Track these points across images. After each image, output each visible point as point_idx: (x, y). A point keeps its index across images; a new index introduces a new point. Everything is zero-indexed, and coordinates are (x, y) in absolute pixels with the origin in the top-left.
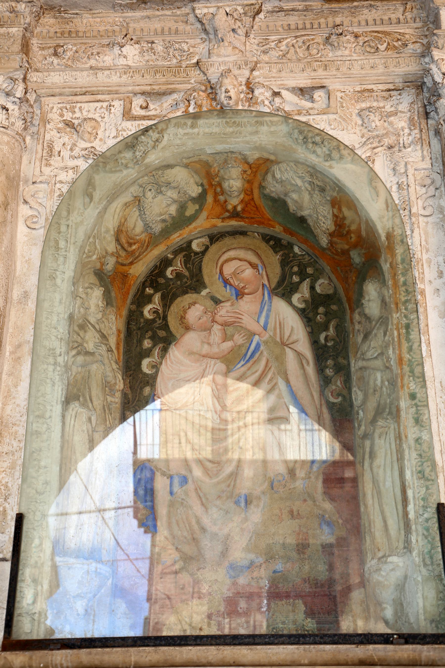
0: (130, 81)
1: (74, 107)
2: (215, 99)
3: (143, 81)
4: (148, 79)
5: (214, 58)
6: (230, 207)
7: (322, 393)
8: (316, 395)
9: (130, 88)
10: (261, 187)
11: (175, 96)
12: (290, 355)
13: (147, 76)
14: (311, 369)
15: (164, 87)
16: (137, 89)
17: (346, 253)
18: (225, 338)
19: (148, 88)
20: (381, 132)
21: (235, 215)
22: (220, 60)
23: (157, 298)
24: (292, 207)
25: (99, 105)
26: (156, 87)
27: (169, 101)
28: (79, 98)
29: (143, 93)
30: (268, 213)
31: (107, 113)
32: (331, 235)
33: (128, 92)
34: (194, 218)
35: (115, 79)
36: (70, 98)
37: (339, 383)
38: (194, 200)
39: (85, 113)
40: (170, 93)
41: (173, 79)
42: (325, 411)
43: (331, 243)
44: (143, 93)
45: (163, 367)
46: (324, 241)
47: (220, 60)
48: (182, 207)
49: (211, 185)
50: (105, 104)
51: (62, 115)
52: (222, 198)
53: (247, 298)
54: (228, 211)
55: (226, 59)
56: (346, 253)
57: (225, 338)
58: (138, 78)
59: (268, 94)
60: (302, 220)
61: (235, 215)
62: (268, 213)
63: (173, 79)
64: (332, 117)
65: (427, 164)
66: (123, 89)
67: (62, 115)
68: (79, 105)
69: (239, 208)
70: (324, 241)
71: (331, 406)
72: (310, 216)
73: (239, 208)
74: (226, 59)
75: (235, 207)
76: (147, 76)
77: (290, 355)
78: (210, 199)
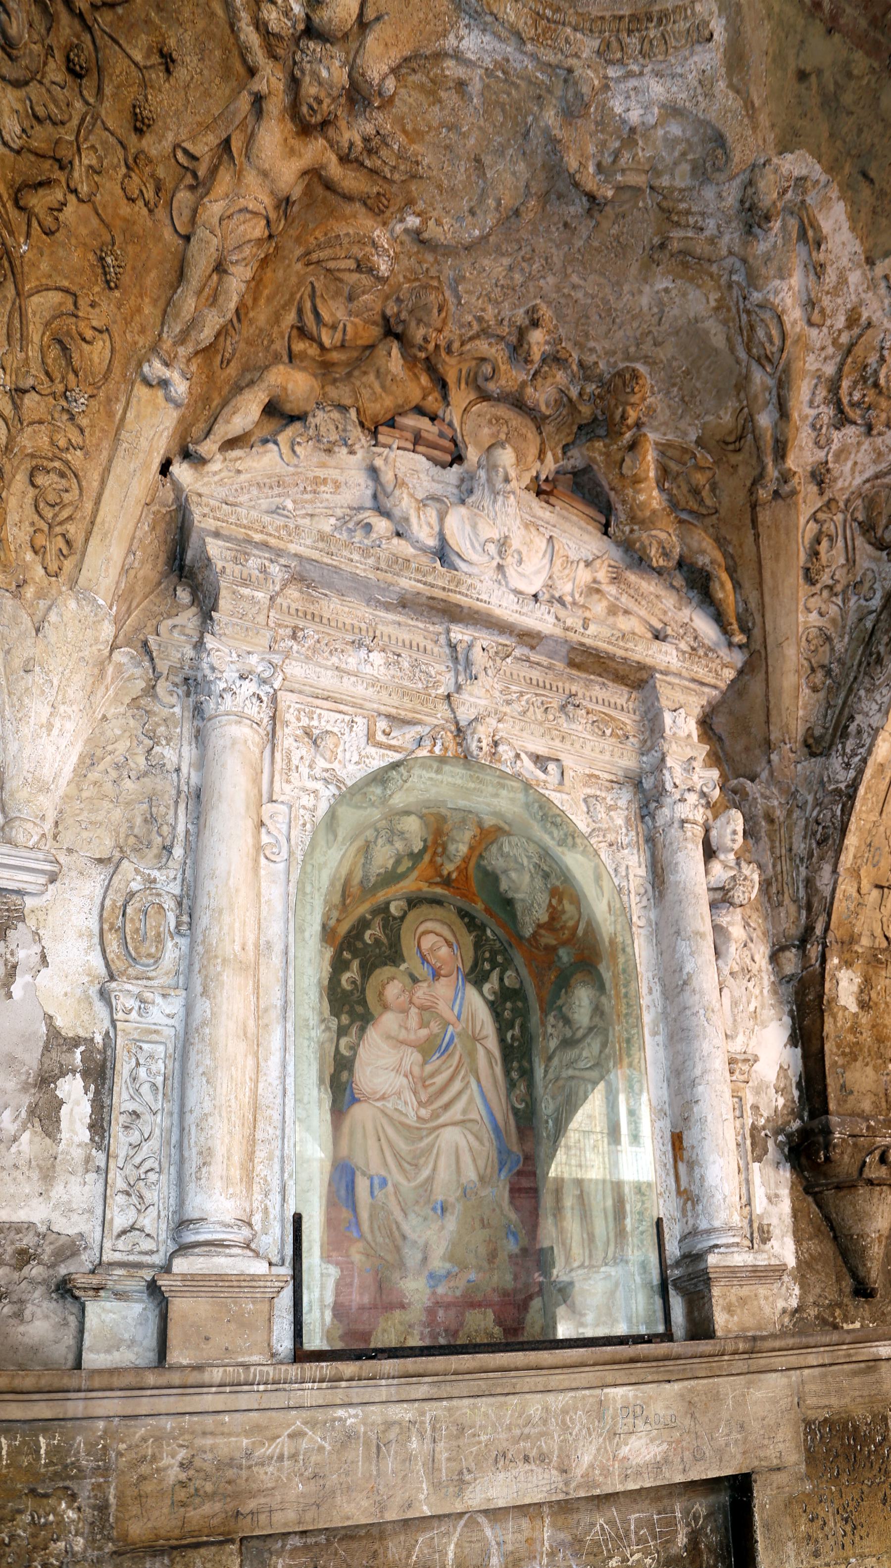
0: (375, 697)
1: (313, 712)
2: (460, 744)
3: (389, 701)
4: (395, 700)
5: (465, 696)
6: (445, 873)
7: (508, 1096)
8: (503, 1100)
9: (375, 706)
10: (481, 856)
11: (419, 728)
12: (481, 1052)
13: (394, 696)
14: (499, 1070)
15: (410, 715)
16: (383, 709)
17: (551, 950)
18: (423, 1024)
19: (393, 711)
20: (604, 826)
21: (447, 882)
22: (472, 700)
23: (355, 964)
24: (504, 885)
25: (340, 716)
26: (403, 713)
27: (412, 732)
28: (319, 702)
29: (388, 716)
30: (474, 886)
31: (347, 730)
32: (539, 926)
33: (373, 710)
34: (404, 876)
35: (360, 690)
36: (310, 699)
37: (522, 1088)
38: (411, 855)
39: (323, 723)
40: (415, 724)
41: (419, 707)
42: (511, 1117)
43: (535, 935)
44: (388, 716)
45: (361, 1050)
46: (528, 931)
47: (472, 700)
48: (398, 862)
49: (435, 842)
50: (347, 718)
51: (299, 720)
52: (439, 860)
53: (443, 980)
54: (441, 876)
55: (478, 701)
56: (551, 950)
57: (423, 1024)
58: (384, 694)
59: (512, 754)
60: (508, 903)
61: (447, 882)
62: (474, 886)
63: (419, 707)
64: (565, 797)
65: (642, 872)
66: (368, 705)
67: (299, 720)
68: (318, 711)
69: (454, 876)
70: (528, 931)
71: (516, 1112)
72: (523, 900)
73: (454, 876)
74: (478, 701)
75: (449, 874)
76: (394, 696)
77: (481, 1053)
78: (427, 858)
